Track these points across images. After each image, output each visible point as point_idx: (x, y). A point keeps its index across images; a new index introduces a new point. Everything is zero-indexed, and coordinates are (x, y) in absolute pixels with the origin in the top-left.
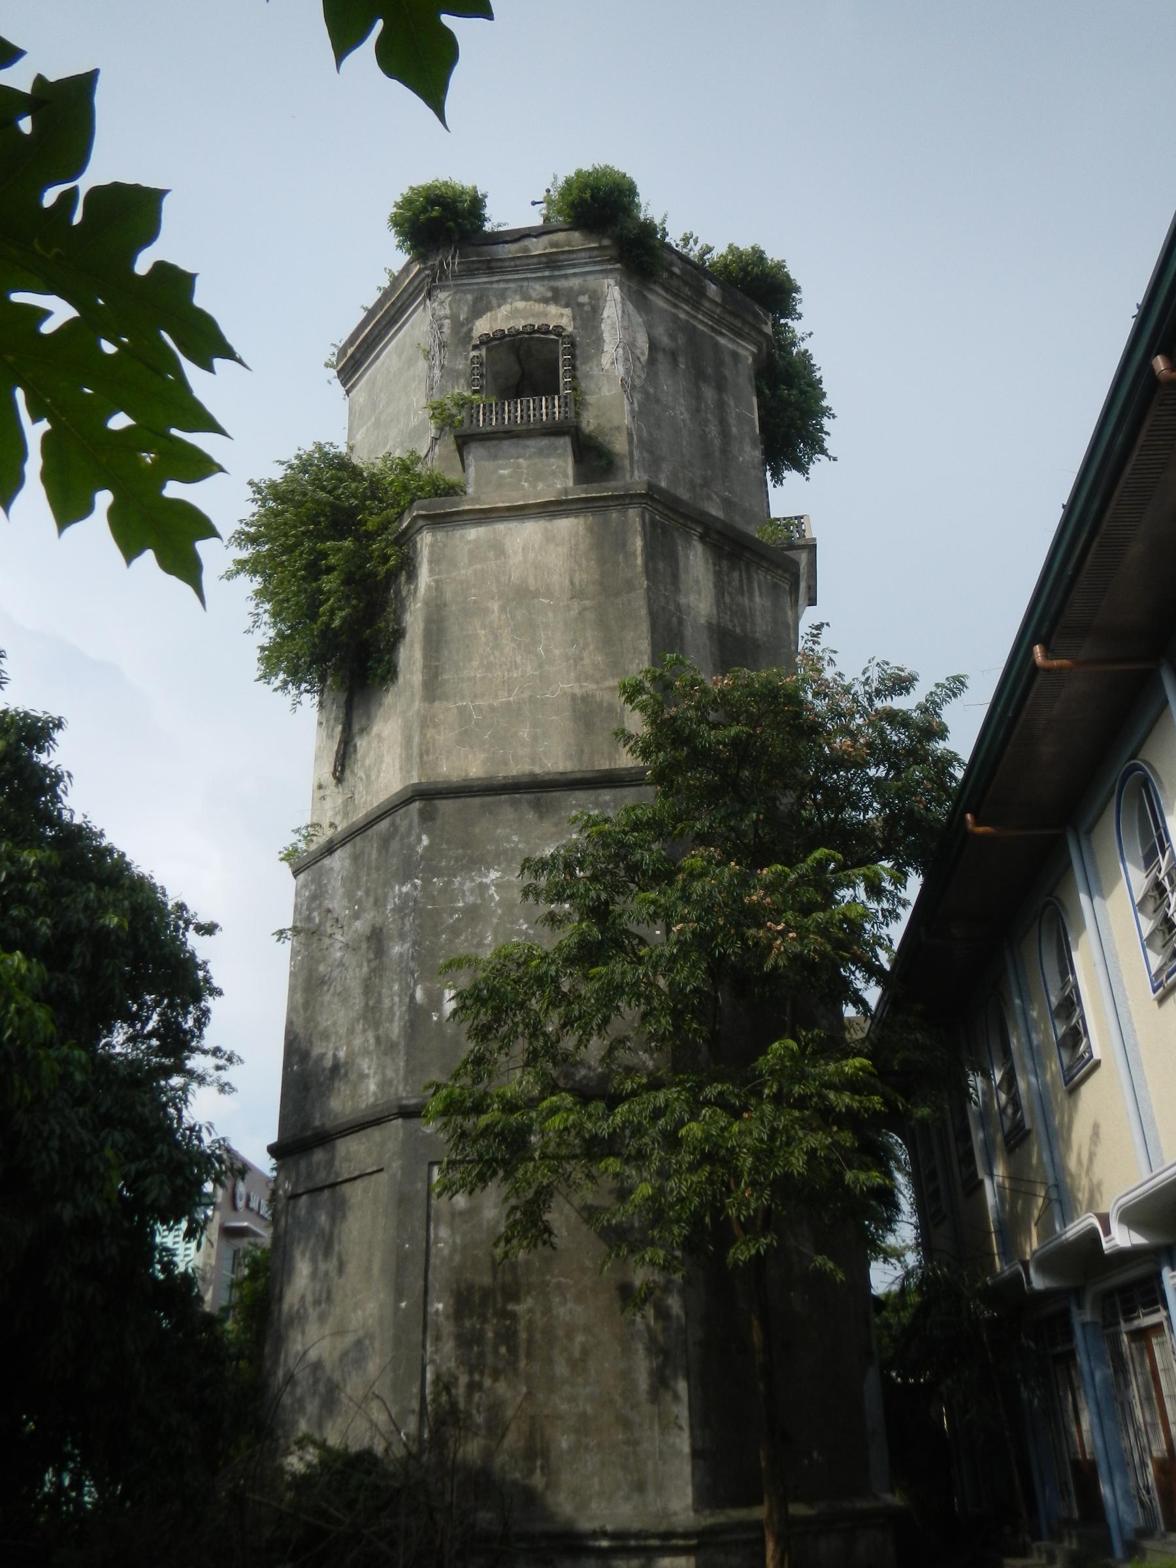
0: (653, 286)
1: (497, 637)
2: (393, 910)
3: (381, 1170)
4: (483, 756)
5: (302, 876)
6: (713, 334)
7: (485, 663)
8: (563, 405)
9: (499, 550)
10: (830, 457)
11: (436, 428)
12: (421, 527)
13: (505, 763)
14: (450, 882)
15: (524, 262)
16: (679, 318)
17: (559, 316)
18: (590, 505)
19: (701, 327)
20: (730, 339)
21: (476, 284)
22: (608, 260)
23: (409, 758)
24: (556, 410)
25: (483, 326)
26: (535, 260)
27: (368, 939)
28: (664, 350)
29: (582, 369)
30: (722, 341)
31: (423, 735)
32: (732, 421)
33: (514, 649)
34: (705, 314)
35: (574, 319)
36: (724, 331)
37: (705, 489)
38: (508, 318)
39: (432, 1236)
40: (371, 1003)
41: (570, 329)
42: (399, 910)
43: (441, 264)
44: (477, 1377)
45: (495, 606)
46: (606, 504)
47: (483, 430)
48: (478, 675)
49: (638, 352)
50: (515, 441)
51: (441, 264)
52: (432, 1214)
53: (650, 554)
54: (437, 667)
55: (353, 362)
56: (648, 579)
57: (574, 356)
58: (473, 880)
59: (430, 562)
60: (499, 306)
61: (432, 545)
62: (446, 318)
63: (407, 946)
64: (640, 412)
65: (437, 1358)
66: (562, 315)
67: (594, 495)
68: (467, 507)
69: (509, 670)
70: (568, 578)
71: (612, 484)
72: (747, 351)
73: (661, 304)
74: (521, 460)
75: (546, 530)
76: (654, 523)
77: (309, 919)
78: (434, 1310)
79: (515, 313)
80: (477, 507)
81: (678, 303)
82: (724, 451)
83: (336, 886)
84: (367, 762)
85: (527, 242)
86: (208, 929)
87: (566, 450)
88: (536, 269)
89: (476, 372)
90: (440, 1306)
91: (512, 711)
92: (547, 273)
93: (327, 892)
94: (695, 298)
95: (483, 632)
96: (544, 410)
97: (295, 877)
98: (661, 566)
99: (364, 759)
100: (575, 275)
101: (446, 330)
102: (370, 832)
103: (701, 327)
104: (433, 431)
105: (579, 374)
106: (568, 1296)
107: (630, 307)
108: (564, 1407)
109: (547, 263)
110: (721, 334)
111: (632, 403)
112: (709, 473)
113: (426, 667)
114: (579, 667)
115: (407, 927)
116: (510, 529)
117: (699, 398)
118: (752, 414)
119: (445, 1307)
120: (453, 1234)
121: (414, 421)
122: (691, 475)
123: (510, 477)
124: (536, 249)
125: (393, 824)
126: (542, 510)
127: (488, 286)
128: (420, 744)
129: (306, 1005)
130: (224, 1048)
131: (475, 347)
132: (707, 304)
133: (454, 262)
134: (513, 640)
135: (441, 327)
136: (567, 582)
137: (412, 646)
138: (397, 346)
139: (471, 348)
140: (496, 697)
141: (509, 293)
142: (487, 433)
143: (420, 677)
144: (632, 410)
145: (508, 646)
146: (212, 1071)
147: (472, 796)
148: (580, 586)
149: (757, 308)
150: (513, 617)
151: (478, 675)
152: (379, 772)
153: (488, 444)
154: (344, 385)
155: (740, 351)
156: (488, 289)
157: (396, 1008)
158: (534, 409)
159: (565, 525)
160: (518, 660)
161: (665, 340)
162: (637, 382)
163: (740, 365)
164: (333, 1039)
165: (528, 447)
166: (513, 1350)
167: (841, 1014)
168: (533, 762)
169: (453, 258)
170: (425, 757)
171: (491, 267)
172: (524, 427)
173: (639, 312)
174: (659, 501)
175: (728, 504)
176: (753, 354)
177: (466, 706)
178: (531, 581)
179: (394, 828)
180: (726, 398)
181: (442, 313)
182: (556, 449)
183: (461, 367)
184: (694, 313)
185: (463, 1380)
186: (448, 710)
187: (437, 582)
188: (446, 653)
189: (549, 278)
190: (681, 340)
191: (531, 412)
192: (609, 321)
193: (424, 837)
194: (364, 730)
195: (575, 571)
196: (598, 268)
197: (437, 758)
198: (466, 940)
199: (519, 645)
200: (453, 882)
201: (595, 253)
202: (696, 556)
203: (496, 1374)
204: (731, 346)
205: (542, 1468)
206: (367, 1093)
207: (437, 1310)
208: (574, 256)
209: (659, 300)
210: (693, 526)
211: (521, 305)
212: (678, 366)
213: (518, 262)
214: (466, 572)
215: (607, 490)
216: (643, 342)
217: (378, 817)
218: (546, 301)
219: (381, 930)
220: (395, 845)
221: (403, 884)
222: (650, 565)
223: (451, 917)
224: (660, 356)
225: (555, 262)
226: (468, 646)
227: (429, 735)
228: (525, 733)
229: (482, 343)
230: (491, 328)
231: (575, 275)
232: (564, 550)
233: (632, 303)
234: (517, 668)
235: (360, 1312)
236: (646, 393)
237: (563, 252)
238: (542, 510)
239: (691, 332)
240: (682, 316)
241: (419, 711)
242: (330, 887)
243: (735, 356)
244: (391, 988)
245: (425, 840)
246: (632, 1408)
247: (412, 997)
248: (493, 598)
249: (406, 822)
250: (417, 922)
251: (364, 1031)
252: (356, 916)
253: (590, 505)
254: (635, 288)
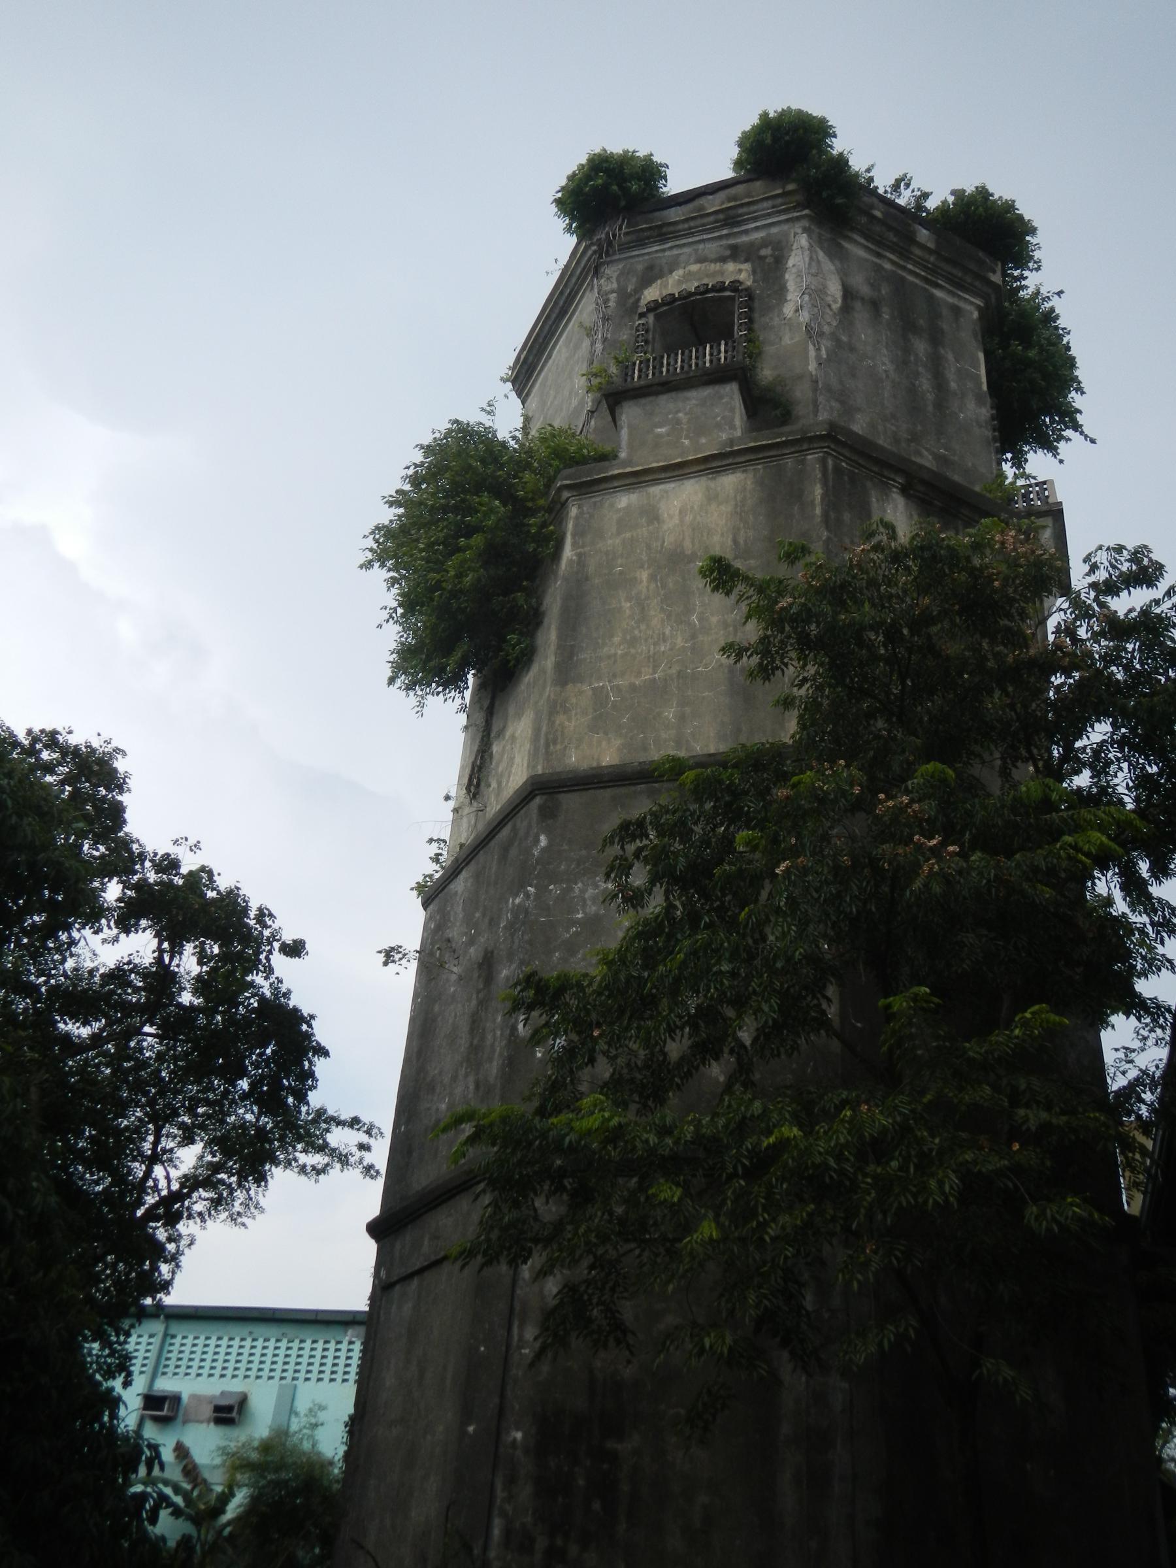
0: (850, 234)
1: (643, 608)
2: (505, 927)
4: (618, 742)
5: (431, 907)
6: (927, 287)
7: (628, 637)
8: (730, 349)
9: (652, 515)
10: (1086, 437)
11: (593, 401)
12: (568, 499)
13: (645, 749)
14: (571, 889)
15: (699, 222)
16: (883, 268)
17: (739, 272)
18: (761, 456)
19: (911, 278)
20: (950, 292)
21: (648, 254)
22: (794, 208)
23: (536, 750)
24: (722, 355)
25: (652, 294)
26: (712, 218)
27: (480, 965)
28: (863, 299)
29: (760, 321)
30: (938, 293)
31: (551, 723)
32: (951, 375)
33: (663, 621)
34: (916, 263)
35: (754, 272)
36: (940, 282)
37: (913, 444)
38: (680, 282)
39: (516, 1338)
40: (475, 1042)
41: (749, 283)
42: (511, 926)
43: (608, 234)
44: (559, 1542)
45: (644, 575)
46: (779, 453)
47: (637, 385)
48: (620, 652)
49: (829, 299)
50: (674, 394)
51: (608, 234)
52: (517, 1306)
53: (832, 503)
54: (572, 646)
55: (526, 367)
56: (828, 528)
57: (751, 309)
58: (597, 887)
59: (574, 536)
60: (671, 272)
61: (577, 518)
62: (613, 291)
63: (514, 966)
64: (829, 359)
65: (509, 1508)
66: (740, 271)
67: (764, 443)
68: (616, 472)
69: (654, 644)
70: (731, 536)
71: (786, 429)
72: (972, 307)
73: (861, 253)
74: (681, 415)
75: (708, 489)
76: (838, 470)
77: (432, 954)
78: (511, 1439)
79: (689, 276)
80: (629, 470)
81: (880, 251)
82: (940, 405)
83: (458, 911)
84: (500, 769)
85: (702, 201)
86: (295, 949)
87: (732, 398)
88: (714, 228)
89: (640, 339)
90: (519, 1435)
91: (657, 690)
92: (725, 232)
93: (449, 920)
94: (901, 244)
95: (629, 604)
96: (708, 357)
97: (425, 909)
98: (847, 517)
99: (497, 766)
100: (757, 228)
101: (611, 304)
102: (492, 843)
103: (911, 278)
104: (590, 404)
105: (756, 326)
107: (821, 254)
109: (725, 220)
110: (937, 286)
111: (818, 350)
112: (919, 428)
113: (559, 647)
114: (739, 634)
115: (515, 946)
116: (667, 492)
117: (907, 350)
118: (977, 368)
119: (524, 1437)
121: (575, 402)
122: (894, 428)
123: (668, 435)
124: (714, 206)
125: (515, 830)
126: (703, 467)
127: (660, 255)
128: (547, 734)
129: (420, 1053)
130: (362, 1118)
131: (642, 315)
132: (918, 252)
133: (619, 229)
134: (662, 610)
135: (606, 301)
136: (730, 542)
137: (549, 629)
138: (567, 337)
139: (637, 318)
140: (639, 673)
141: (682, 258)
142: (641, 388)
143: (553, 658)
144: (818, 357)
145: (656, 617)
146: (354, 1150)
147: (601, 788)
148: (745, 541)
149: (981, 254)
150: (664, 586)
151: (620, 652)
152: (509, 777)
153: (643, 401)
154: (519, 396)
155: (962, 304)
156: (660, 257)
157: (497, 1044)
158: (697, 358)
159: (730, 482)
160: (667, 631)
161: (865, 290)
162: (826, 329)
163: (962, 320)
164: (438, 1091)
165: (688, 399)
168: (678, 743)
169: (620, 229)
170: (552, 748)
171: (663, 234)
172: (683, 376)
173: (831, 260)
174: (844, 444)
175: (938, 458)
176: (978, 307)
177: (603, 687)
178: (687, 544)
179: (515, 830)
180: (942, 351)
181: (608, 288)
182: (721, 398)
183: (625, 337)
184: (902, 263)
185: (541, 1543)
186: (581, 692)
187: (580, 555)
188: (584, 630)
189: (727, 236)
190: (885, 290)
191: (694, 361)
192: (794, 270)
193: (543, 838)
194: (501, 733)
195: (739, 529)
196: (784, 217)
197: (566, 747)
198: (584, 959)
199: (669, 616)
200: (573, 889)
201: (779, 201)
202: (895, 508)
204: (950, 300)
207: (515, 1439)
208: (755, 207)
209: (857, 250)
210: (892, 476)
211: (694, 268)
212: (880, 316)
213: (692, 224)
214: (613, 542)
215: (780, 435)
216: (834, 289)
217: (500, 823)
218: (723, 260)
219: (492, 952)
220: (513, 852)
221: (517, 895)
222: (832, 515)
223: (568, 932)
224: (858, 305)
225: (733, 218)
226: (609, 622)
227: (557, 722)
228: (670, 714)
229: (649, 310)
230: (661, 294)
231: (757, 228)
232: (727, 508)
233: (822, 249)
234: (665, 641)
235: (429, 1437)
236: (838, 341)
237: (742, 205)
238: (703, 467)
239: (899, 285)
240: (888, 266)
241: (549, 696)
242: (452, 913)
243: (957, 311)
244: (494, 1021)
245: (543, 841)
247: (514, 1028)
248: (642, 567)
249: (525, 823)
250: (526, 937)
251: (466, 1075)
252: (472, 941)
253: (761, 456)
254: (828, 236)
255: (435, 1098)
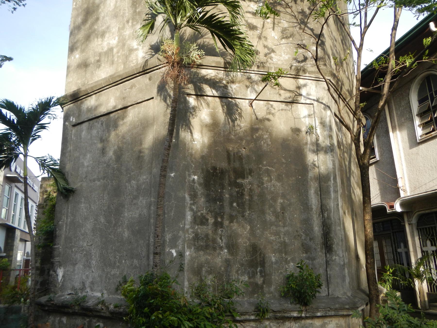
3: (153, 98)
44: (219, 220)
78: (192, 179)
90: (196, 177)
106: (272, 177)
108: (273, 238)
120: (202, 137)
166: (241, 205)
167: (422, 41)
185: (211, 221)
203: (232, 219)
205: (261, 272)
206: (137, 59)
207: (194, 179)
246: (311, 239)
255: (106, 39)
